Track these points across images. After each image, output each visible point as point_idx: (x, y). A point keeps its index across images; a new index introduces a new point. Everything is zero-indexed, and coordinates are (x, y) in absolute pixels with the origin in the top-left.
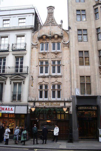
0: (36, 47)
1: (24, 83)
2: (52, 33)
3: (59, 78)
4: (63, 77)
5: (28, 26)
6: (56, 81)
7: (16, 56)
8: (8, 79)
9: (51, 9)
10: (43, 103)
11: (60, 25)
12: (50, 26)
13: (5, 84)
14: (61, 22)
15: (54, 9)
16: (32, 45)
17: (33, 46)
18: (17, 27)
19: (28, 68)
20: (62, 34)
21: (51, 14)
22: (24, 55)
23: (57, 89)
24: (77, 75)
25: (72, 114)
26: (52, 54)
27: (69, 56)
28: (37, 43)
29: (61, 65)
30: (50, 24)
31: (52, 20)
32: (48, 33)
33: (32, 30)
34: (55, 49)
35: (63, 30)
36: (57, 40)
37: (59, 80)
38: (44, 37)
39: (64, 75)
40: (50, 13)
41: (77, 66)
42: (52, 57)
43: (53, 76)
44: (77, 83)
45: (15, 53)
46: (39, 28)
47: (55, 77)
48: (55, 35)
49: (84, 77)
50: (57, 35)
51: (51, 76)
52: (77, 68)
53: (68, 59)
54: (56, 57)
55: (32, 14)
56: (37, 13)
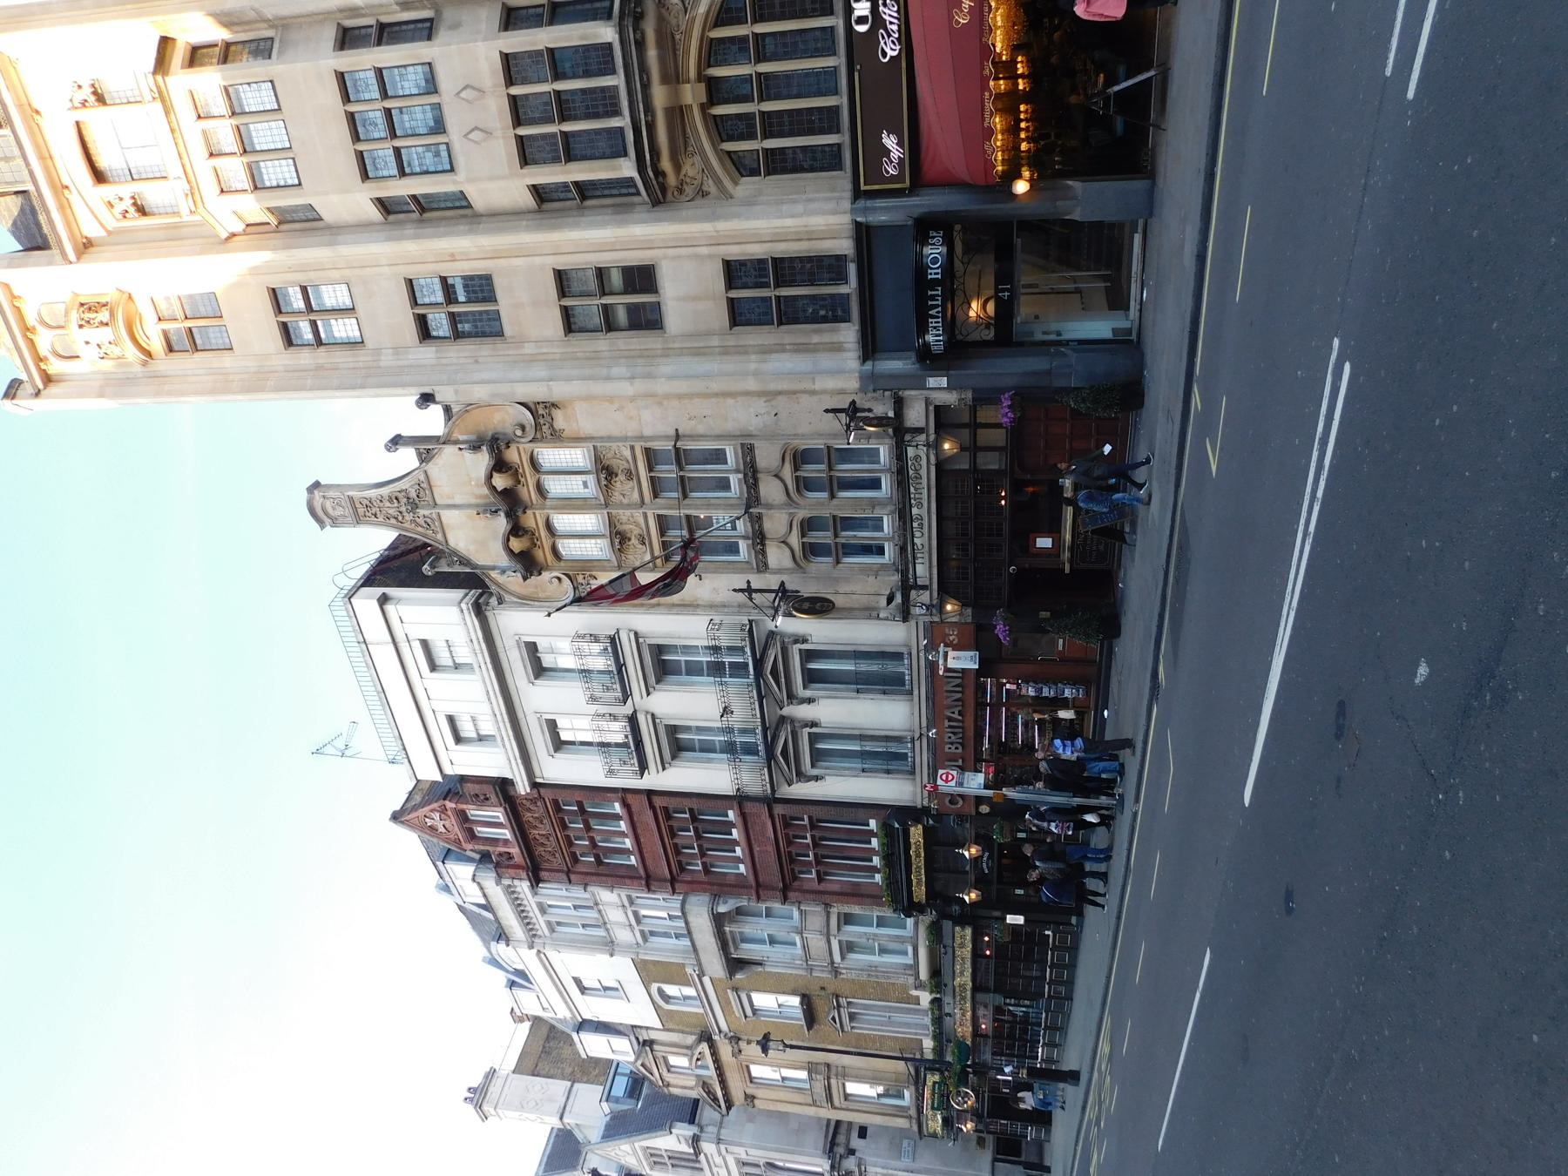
1: (805, 641)
7: (652, 679)
8: (787, 711)
11: (419, 454)
13: (814, 724)
15: (317, 485)
20: (475, 447)
22: (641, 640)
23: (823, 467)
24: (725, 351)
25: (974, 391)
26: (617, 497)
28: (559, 579)
29: (677, 450)
37: (767, 456)
40: (355, 509)
41: (667, 353)
44: (780, 348)
45: (637, 686)
47: (756, 480)
48: (494, 487)
51: (748, 507)
52: (682, 352)
55: (389, 608)
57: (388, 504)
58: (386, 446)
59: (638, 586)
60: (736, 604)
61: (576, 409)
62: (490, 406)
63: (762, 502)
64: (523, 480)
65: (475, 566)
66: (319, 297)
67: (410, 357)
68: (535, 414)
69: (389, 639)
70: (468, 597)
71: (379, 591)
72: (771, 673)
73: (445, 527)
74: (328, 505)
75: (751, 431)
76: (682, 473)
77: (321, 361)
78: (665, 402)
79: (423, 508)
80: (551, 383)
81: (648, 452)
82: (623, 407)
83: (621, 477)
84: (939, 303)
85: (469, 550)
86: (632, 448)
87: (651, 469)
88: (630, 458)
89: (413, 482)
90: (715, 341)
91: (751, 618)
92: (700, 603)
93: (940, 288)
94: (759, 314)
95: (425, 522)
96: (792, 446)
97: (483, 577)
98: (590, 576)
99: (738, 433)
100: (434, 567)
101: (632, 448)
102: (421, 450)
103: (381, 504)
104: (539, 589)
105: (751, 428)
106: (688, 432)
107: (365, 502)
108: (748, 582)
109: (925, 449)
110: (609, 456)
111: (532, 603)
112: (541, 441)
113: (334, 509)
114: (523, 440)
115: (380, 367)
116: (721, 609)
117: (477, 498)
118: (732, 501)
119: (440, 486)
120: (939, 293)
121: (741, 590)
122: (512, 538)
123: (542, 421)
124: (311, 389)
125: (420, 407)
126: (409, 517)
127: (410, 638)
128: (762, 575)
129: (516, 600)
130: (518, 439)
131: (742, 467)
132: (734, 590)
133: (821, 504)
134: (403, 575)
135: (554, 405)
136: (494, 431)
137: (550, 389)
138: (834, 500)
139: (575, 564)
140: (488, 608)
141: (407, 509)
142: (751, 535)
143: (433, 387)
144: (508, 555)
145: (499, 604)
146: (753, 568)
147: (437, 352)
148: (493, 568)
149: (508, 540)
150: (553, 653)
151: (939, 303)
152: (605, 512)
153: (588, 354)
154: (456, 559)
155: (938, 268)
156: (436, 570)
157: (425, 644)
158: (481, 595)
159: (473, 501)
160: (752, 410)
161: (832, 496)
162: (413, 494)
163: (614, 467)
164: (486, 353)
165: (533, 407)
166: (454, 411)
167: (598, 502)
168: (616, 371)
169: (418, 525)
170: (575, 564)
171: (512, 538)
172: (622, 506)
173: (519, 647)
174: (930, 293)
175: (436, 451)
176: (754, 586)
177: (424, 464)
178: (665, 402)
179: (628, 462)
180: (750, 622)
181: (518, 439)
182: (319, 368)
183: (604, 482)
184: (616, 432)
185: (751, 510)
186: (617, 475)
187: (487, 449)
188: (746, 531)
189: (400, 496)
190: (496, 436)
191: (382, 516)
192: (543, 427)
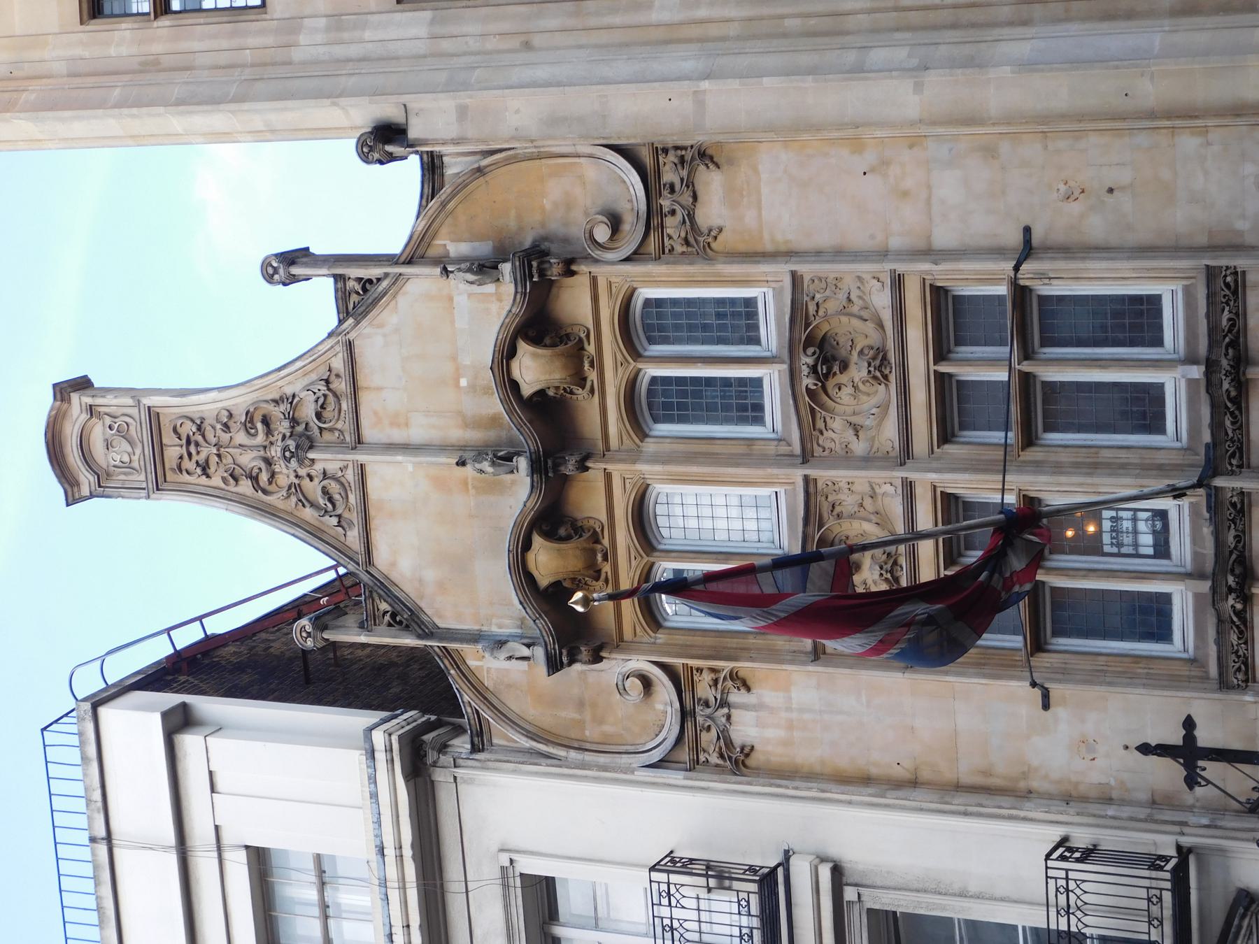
2: (476, 423)
4: (1241, 263)
5: (379, 823)
11: (342, 296)
14: (294, 279)
15: (83, 384)
16: (684, 755)
19: (1088, 854)
20: (484, 268)
21: (169, 438)
22: (850, 894)
26: (837, 433)
27: (857, 145)
28: (647, 683)
29: (1021, 294)
30: (326, 460)
31: (266, 421)
32: (493, 488)
33: (443, 748)
34: (742, 382)
35: (416, 253)
36: (591, 349)
40: (158, 448)
43: (1216, 426)
46: (409, 641)
48: (515, 386)
50: (506, 353)
51: (1212, 468)
55: (190, 742)
56: (159, 650)
57: (241, 437)
58: (265, 265)
59: (850, 592)
60: (1143, 796)
61: (760, 167)
62: (539, 156)
64: (592, 376)
65: (428, 631)
67: (367, 35)
68: (651, 178)
69: (170, 836)
70: (395, 721)
71: (171, 699)
73: (372, 512)
74: (98, 434)
75: (1240, 233)
76: (1026, 367)
77: (157, 48)
78: (1005, 147)
79: (328, 447)
80: (705, 85)
81: (938, 296)
82: (885, 163)
83: (858, 371)
85: (420, 581)
86: (898, 282)
87: (941, 354)
88: (887, 317)
89: (314, 377)
91: (1186, 841)
92: (1035, 784)
95: (325, 491)
97: (444, 664)
98: (734, 676)
99: (1202, 240)
100: (324, 628)
101: (898, 282)
102: (351, 284)
103: (225, 437)
104: (588, 716)
105: (1241, 225)
106: (1059, 237)
107: (188, 428)
108: (1189, 724)
111: (561, 752)
112: (657, 259)
113: (108, 445)
114: (610, 256)
115: (290, 63)
116: (1094, 808)
118: (1161, 458)
119: (379, 389)
121: (1162, 750)
122: (537, 540)
123: (666, 203)
124: (119, 105)
125: (365, 158)
126: (285, 473)
127: (226, 839)
128: (1234, 697)
129: (526, 743)
130: (597, 253)
131: (1203, 347)
132: (1145, 749)
135: (705, 156)
136: (542, 232)
137: (699, 100)
139: (698, 640)
140: (445, 759)
141: (285, 449)
142: (1209, 565)
143: (405, 98)
144: (519, 587)
145: (475, 749)
146: (1206, 678)
147: (433, 22)
148: (474, 638)
149: (527, 545)
150: (596, 927)
152: (798, 475)
153: (813, 22)
154: (384, 606)
157: (260, 860)
158: (429, 727)
159: (457, 434)
162: (308, 411)
163: (842, 340)
164: (553, 23)
165: (647, 157)
166: (450, 171)
167: (784, 449)
168: (878, 56)
169: (306, 501)
170: (698, 640)
171: (537, 540)
172: (847, 459)
173: (506, 886)
175: (385, 284)
176: (1204, 738)
177: (351, 321)
178: (1005, 147)
179: (880, 325)
180: (1184, 853)
181: (597, 253)
182: (150, 66)
183: (808, 382)
184: (859, 237)
185: (1219, 482)
186: (844, 366)
187: (514, 271)
188: (1196, 556)
189: (276, 412)
191: (221, 472)
192: (669, 221)
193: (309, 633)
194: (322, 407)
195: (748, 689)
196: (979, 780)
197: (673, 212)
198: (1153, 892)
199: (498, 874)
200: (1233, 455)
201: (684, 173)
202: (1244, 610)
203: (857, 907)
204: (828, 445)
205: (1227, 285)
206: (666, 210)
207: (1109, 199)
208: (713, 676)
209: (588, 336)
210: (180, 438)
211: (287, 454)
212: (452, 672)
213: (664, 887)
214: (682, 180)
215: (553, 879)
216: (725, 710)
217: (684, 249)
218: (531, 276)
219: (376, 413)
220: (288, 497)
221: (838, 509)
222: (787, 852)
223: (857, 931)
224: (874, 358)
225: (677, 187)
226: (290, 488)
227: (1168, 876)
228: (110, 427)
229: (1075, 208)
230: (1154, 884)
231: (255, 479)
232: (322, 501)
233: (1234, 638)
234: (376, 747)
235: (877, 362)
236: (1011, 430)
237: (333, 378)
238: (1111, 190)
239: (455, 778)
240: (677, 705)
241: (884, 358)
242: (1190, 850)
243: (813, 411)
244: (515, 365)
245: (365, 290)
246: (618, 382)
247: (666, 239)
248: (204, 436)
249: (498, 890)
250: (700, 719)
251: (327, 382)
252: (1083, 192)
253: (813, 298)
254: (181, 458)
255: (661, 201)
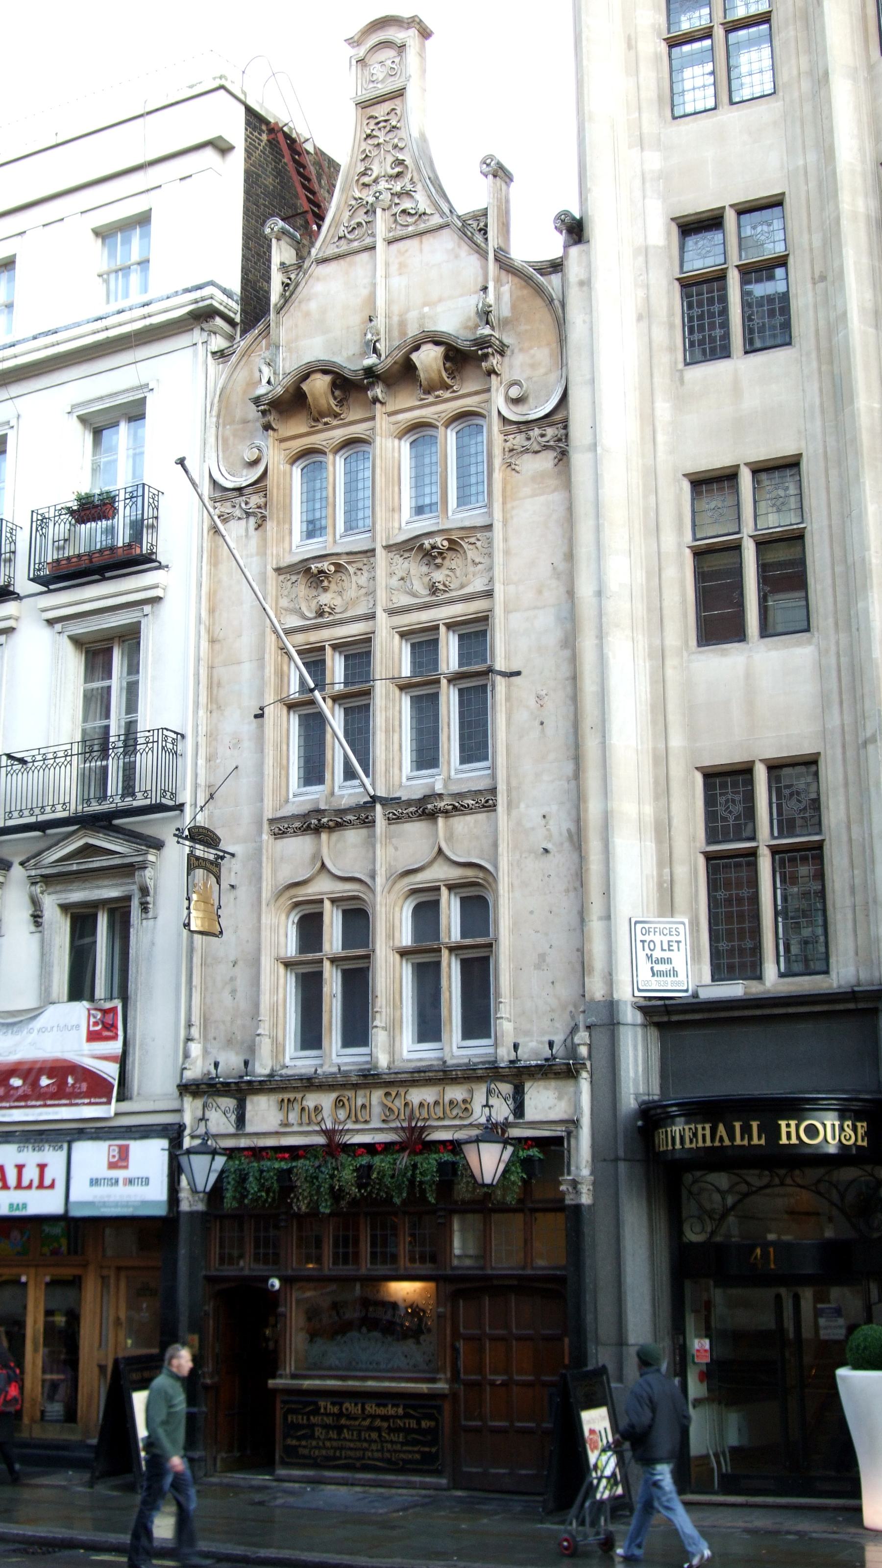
0: (248, 514)
3: (470, 819)
6: (440, 851)
9: (390, 53)
10: (312, 1100)
12: (380, 245)
16: (218, 494)
17: (227, 508)
18: (67, 328)
22: (147, 609)
28: (255, 463)
31: (399, 175)
35: (505, 264)
36: (447, 395)
38: (319, 385)
39: (514, 783)
41: (659, 656)
42: (405, 600)
43: (409, 803)
48: (417, 348)
49: (745, 771)
52: (659, 681)
53: (554, 592)
54: (434, 590)
57: (390, 159)
58: (492, 157)
63: (392, 827)
64: (431, 399)
66: (752, 42)
72: (87, 844)
73: (348, 259)
75: (518, 807)
84: (738, 1142)
85: (309, 300)
90: (677, 741)
91: (188, 809)
93: (763, 1142)
94: (724, 819)
96: (491, 880)
105: (522, 806)
109: (483, 1120)
110: (471, 554)
117: (401, 316)
119: (421, 250)
120: (755, 1141)
122: (328, 378)
125: (558, 217)
133: (391, 936)
134: (269, 181)
138: (397, 957)
141: (380, 193)
145: (214, 353)
149: (325, 372)
151: (738, 1142)
155: (798, 1137)
156: (274, 241)
157: (143, 220)
160: (554, 808)
161: (404, 953)
165: (558, 417)
174: (755, 1125)
179: (462, 586)
183: (427, 543)
190: (508, 353)
191: (368, 148)
192: (523, 435)
193: (272, 229)
194: (409, 214)
195: (256, 529)
196: (215, 680)
197: (529, 439)
198: (149, 793)
199: (143, 383)
200: (394, 814)
201: (552, 443)
202: (311, 829)
203: (140, 614)
204: (394, 561)
205: (487, 801)
206: (531, 433)
207: (537, 723)
208: (263, 504)
209: (454, 392)
210: (388, 114)
211: (378, 194)
212: (256, 331)
213: (135, 495)
214: (548, 442)
215: (144, 418)
216: (245, 516)
217: (507, 449)
218: (481, 349)
219: (407, 251)
220: (356, 199)
221: (359, 573)
222: (167, 567)
223: (124, 617)
224: (444, 585)
225: (544, 439)
226: (361, 199)
227: (158, 801)
228: (393, 62)
229: (532, 702)
230: (154, 793)
231: (364, 174)
232: (353, 223)
233: (297, 824)
234: (203, 290)
235: (441, 587)
236: (345, 687)
237: (426, 218)
238: (542, 723)
239: (195, 344)
240: (244, 484)
241: (445, 591)
242: (182, 811)
243: (412, 549)
244: (430, 346)
245: (480, 230)
246: (428, 416)
247: (512, 436)
248: (390, 131)
249: (136, 383)
250: (237, 500)
251: (424, 214)
252: (542, 706)
253: (478, 540)
254: (376, 118)
255: (536, 429)
